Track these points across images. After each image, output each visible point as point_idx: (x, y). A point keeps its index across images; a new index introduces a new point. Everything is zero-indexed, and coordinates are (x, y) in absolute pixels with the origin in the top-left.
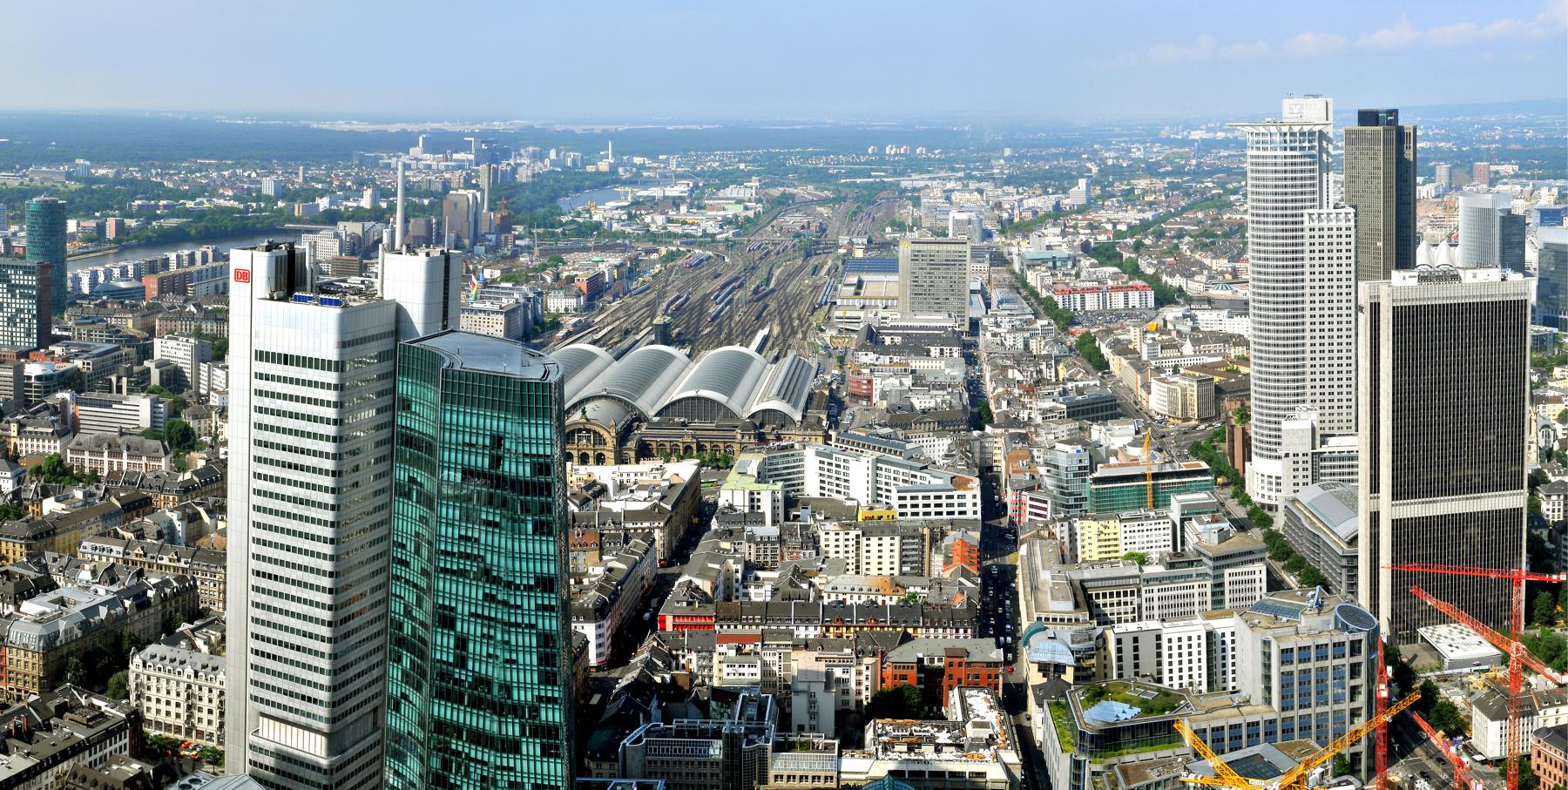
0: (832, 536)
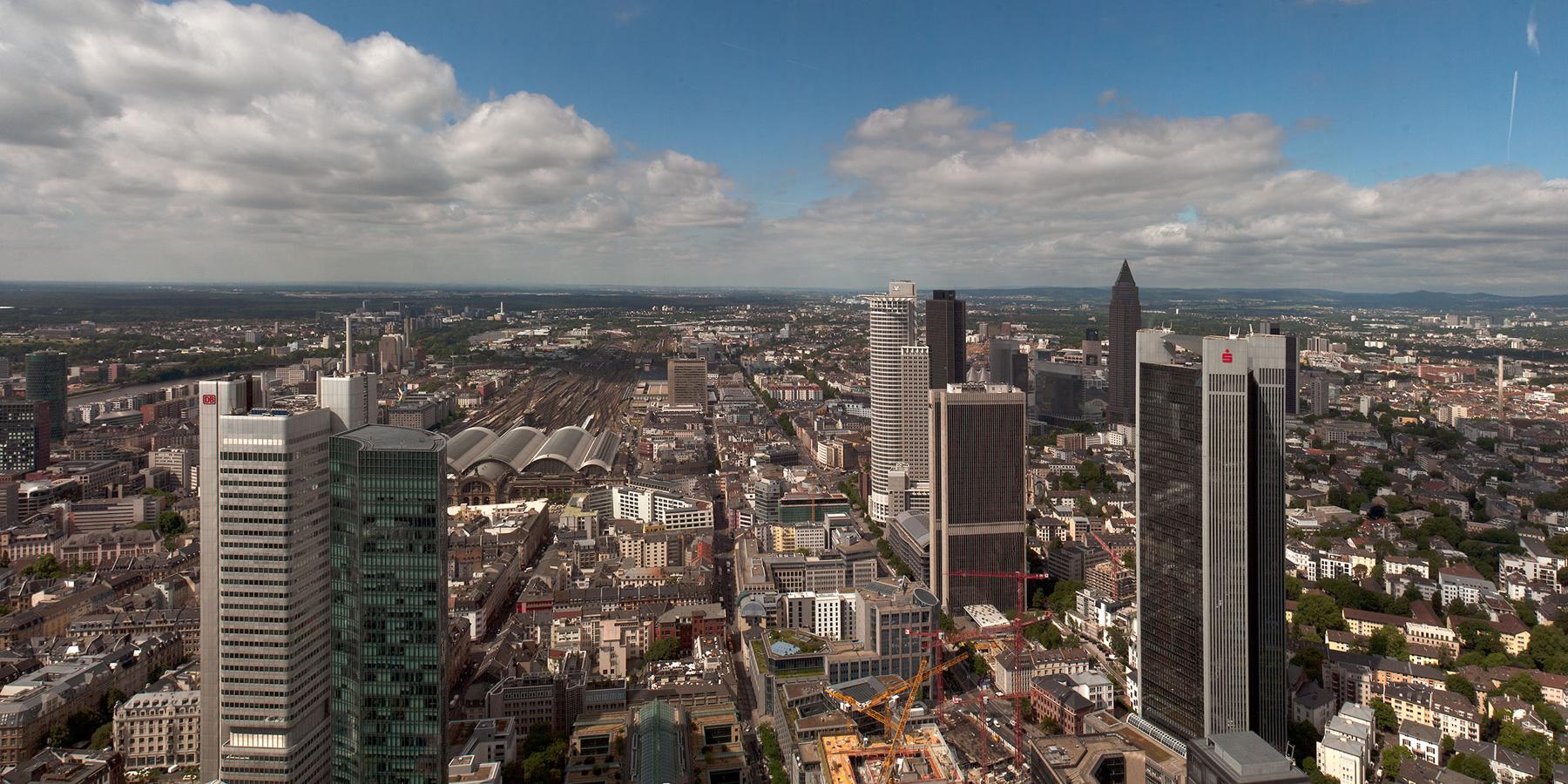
0: (627, 544)
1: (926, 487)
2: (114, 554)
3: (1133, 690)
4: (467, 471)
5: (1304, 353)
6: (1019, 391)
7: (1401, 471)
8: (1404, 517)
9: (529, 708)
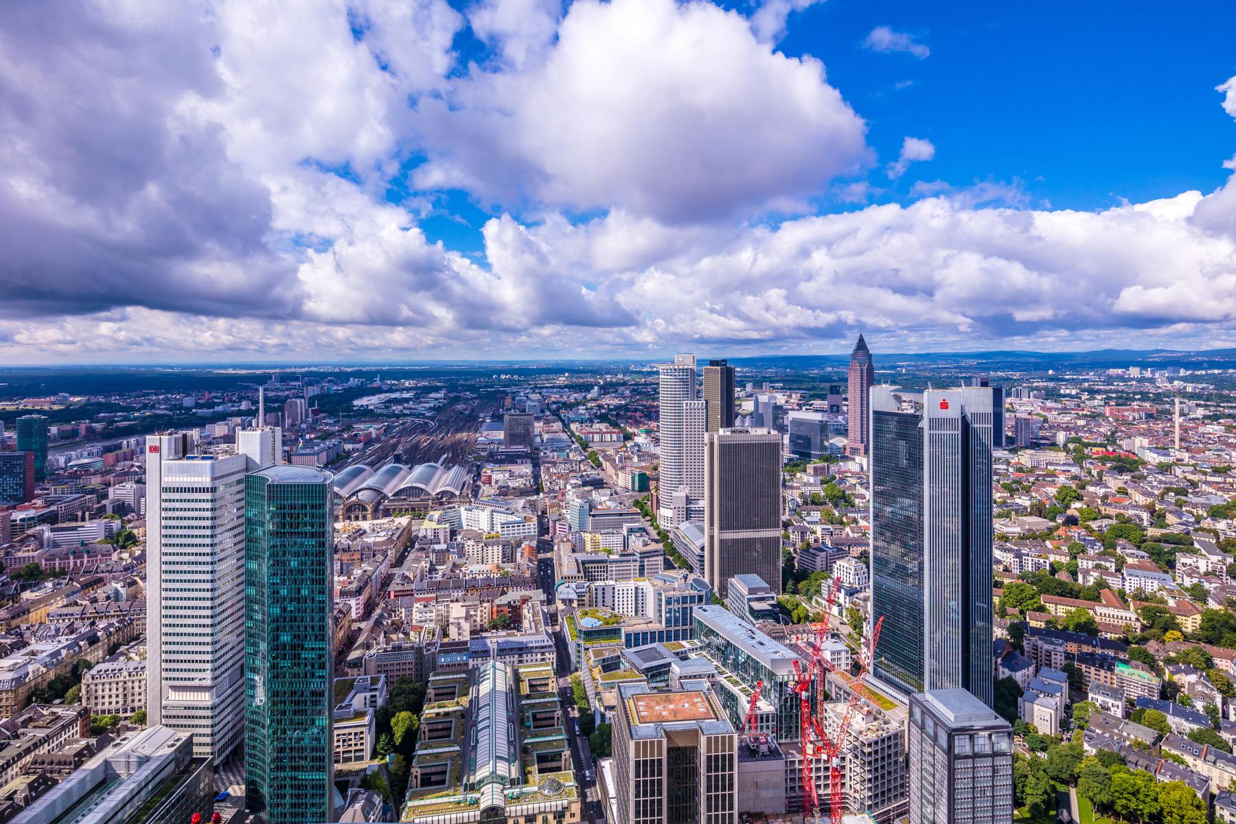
0: (471, 547)
1: (704, 504)
2: (82, 563)
3: (866, 655)
4: (350, 497)
5: (1009, 400)
6: (776, 432)
7: (1091, 489)
8: (1094, 525)
9: (395, 668)
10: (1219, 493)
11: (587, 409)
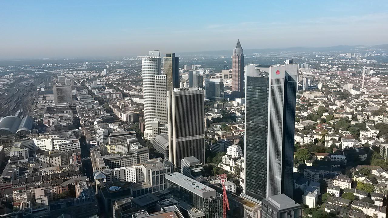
7: (331, 107)
8: (331, 122)
10: (376, 105)
11: (101, 81)
